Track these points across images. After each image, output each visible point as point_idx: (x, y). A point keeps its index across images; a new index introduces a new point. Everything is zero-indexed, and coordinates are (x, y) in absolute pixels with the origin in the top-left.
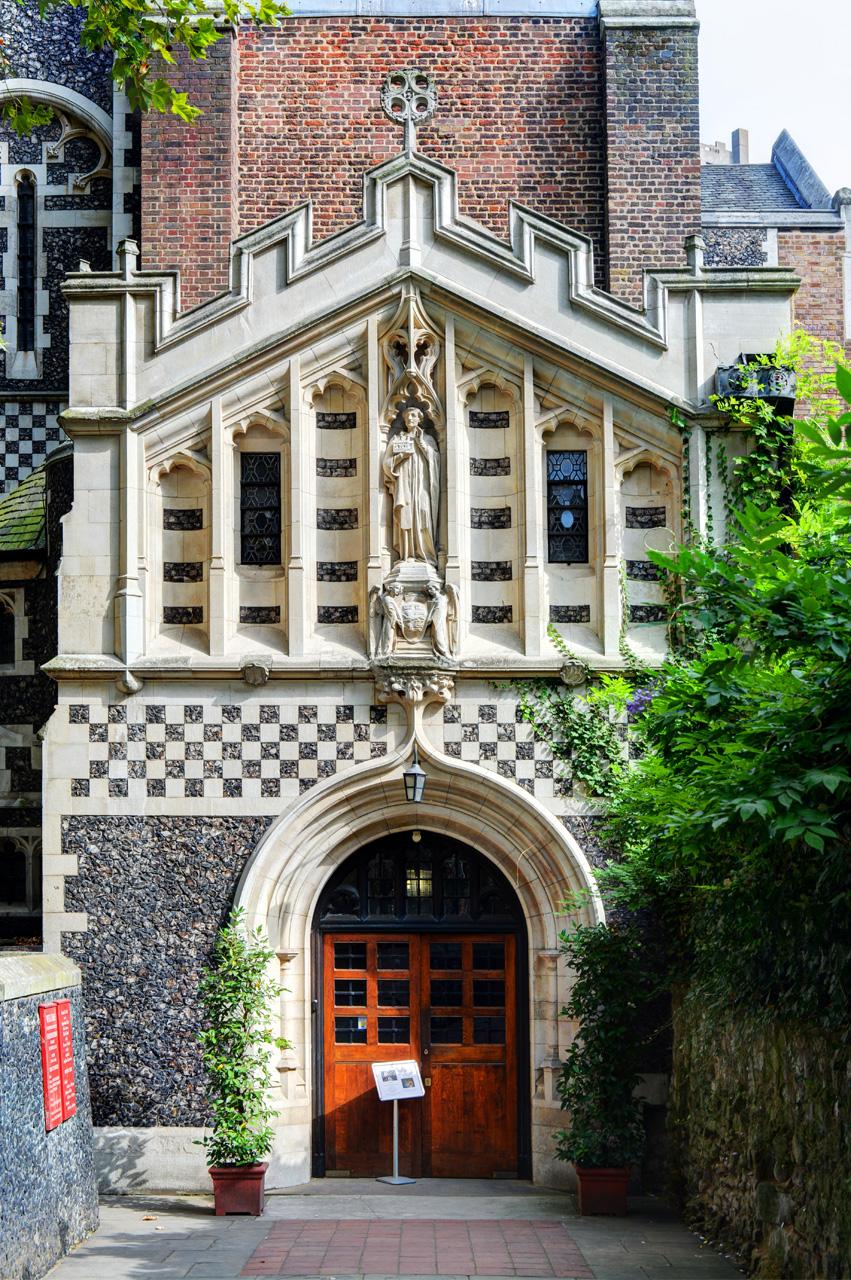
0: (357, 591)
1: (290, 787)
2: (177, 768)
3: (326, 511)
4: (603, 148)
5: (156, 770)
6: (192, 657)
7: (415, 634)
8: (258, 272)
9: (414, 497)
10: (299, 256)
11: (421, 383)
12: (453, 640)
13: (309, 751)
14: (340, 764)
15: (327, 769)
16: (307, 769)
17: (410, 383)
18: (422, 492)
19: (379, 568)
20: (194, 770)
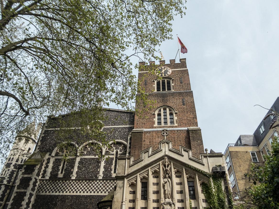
0: (159, 204)
3: (154, 191)
4: (190, 145)
8: (145, 156)
9: (168, 188)
10: (150, 153)
11: (168, 171)
17: (166, 170)
19: (163, 201)
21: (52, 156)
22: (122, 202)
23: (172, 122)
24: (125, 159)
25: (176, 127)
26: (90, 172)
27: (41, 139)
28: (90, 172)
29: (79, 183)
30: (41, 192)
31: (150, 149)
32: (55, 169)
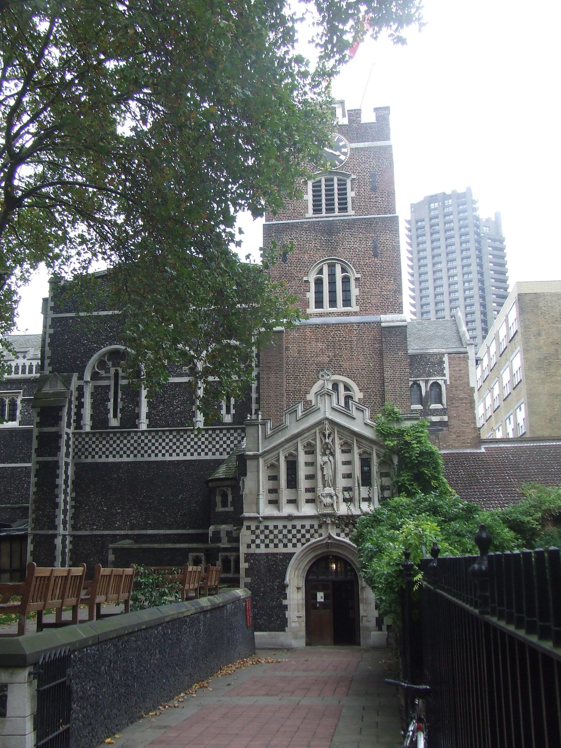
1: (299, 545)
2: (272, 541)
5: (267, 541)
6: (275, 513)
7: (329, 506)
9: (328, 471)
10: (300, 414)
12: (338, 507)
13: (303, 536)
14: (311, 539)
15: (308, 540)
16: (303, 540)
17: (327, 444)
18: (330, 470)
20: (276, 541)
21: (87, 382)
22: (258, 495)
23: (347, 302)
24: (258, 425)
25: (355, 314)
26: (177, 414)
27: (48, 340)
28: (177, 414)
29: (157, 437)
30: (83, 457)
31: (300, 407)
32: (98, 409)
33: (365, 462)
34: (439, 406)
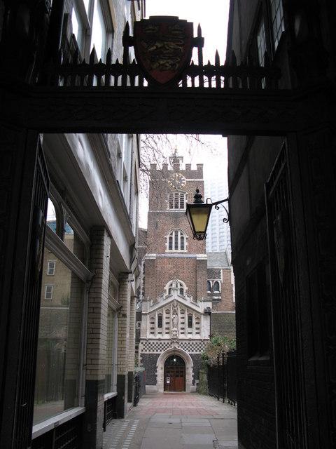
6: (154, 337)
9: (175, 321)
10: (164, 297)
19: (172, 329)
23: (182, 248)
33: (190, 318)
34: (217, 292)
